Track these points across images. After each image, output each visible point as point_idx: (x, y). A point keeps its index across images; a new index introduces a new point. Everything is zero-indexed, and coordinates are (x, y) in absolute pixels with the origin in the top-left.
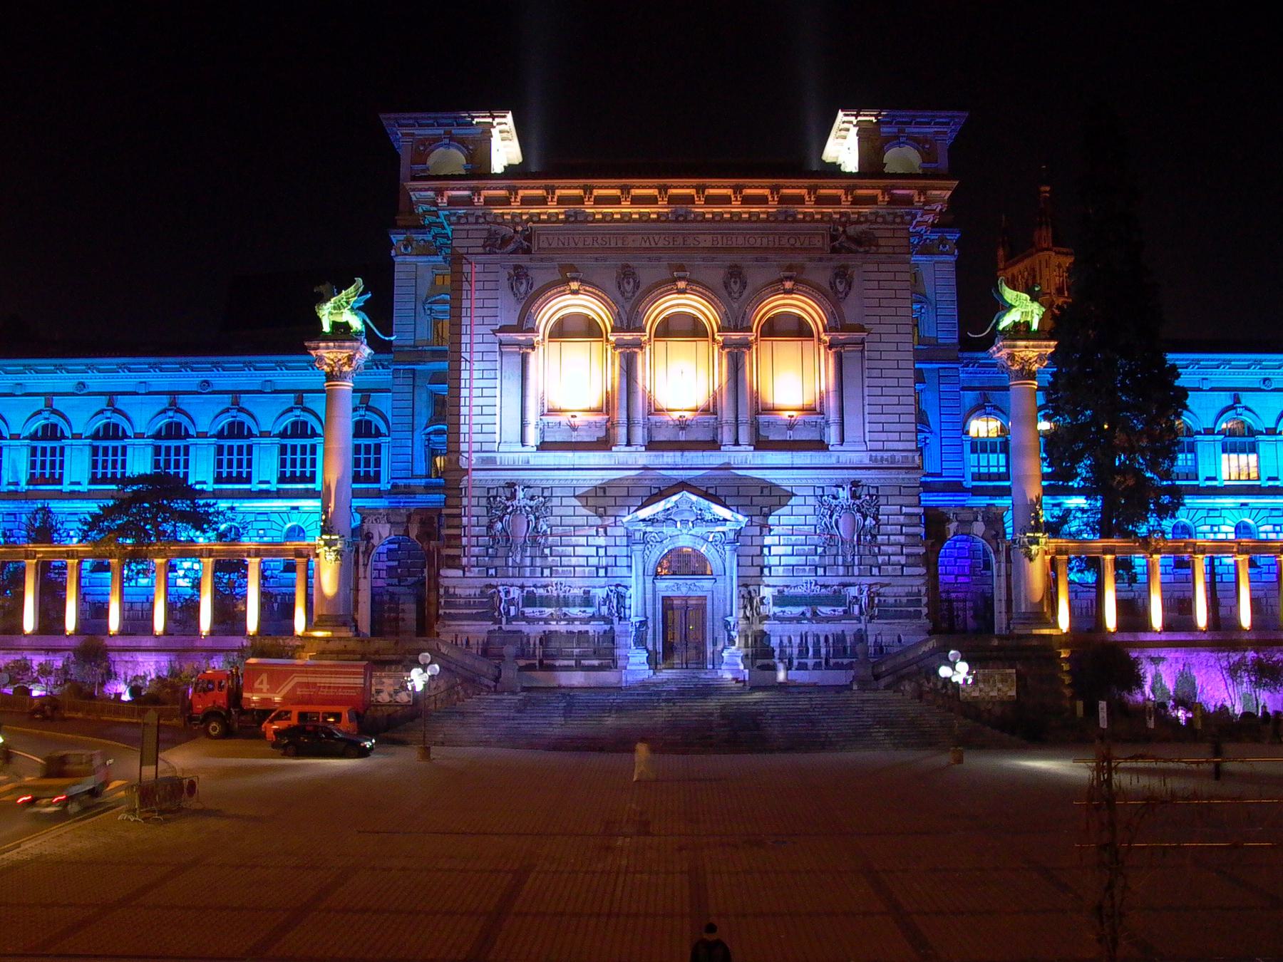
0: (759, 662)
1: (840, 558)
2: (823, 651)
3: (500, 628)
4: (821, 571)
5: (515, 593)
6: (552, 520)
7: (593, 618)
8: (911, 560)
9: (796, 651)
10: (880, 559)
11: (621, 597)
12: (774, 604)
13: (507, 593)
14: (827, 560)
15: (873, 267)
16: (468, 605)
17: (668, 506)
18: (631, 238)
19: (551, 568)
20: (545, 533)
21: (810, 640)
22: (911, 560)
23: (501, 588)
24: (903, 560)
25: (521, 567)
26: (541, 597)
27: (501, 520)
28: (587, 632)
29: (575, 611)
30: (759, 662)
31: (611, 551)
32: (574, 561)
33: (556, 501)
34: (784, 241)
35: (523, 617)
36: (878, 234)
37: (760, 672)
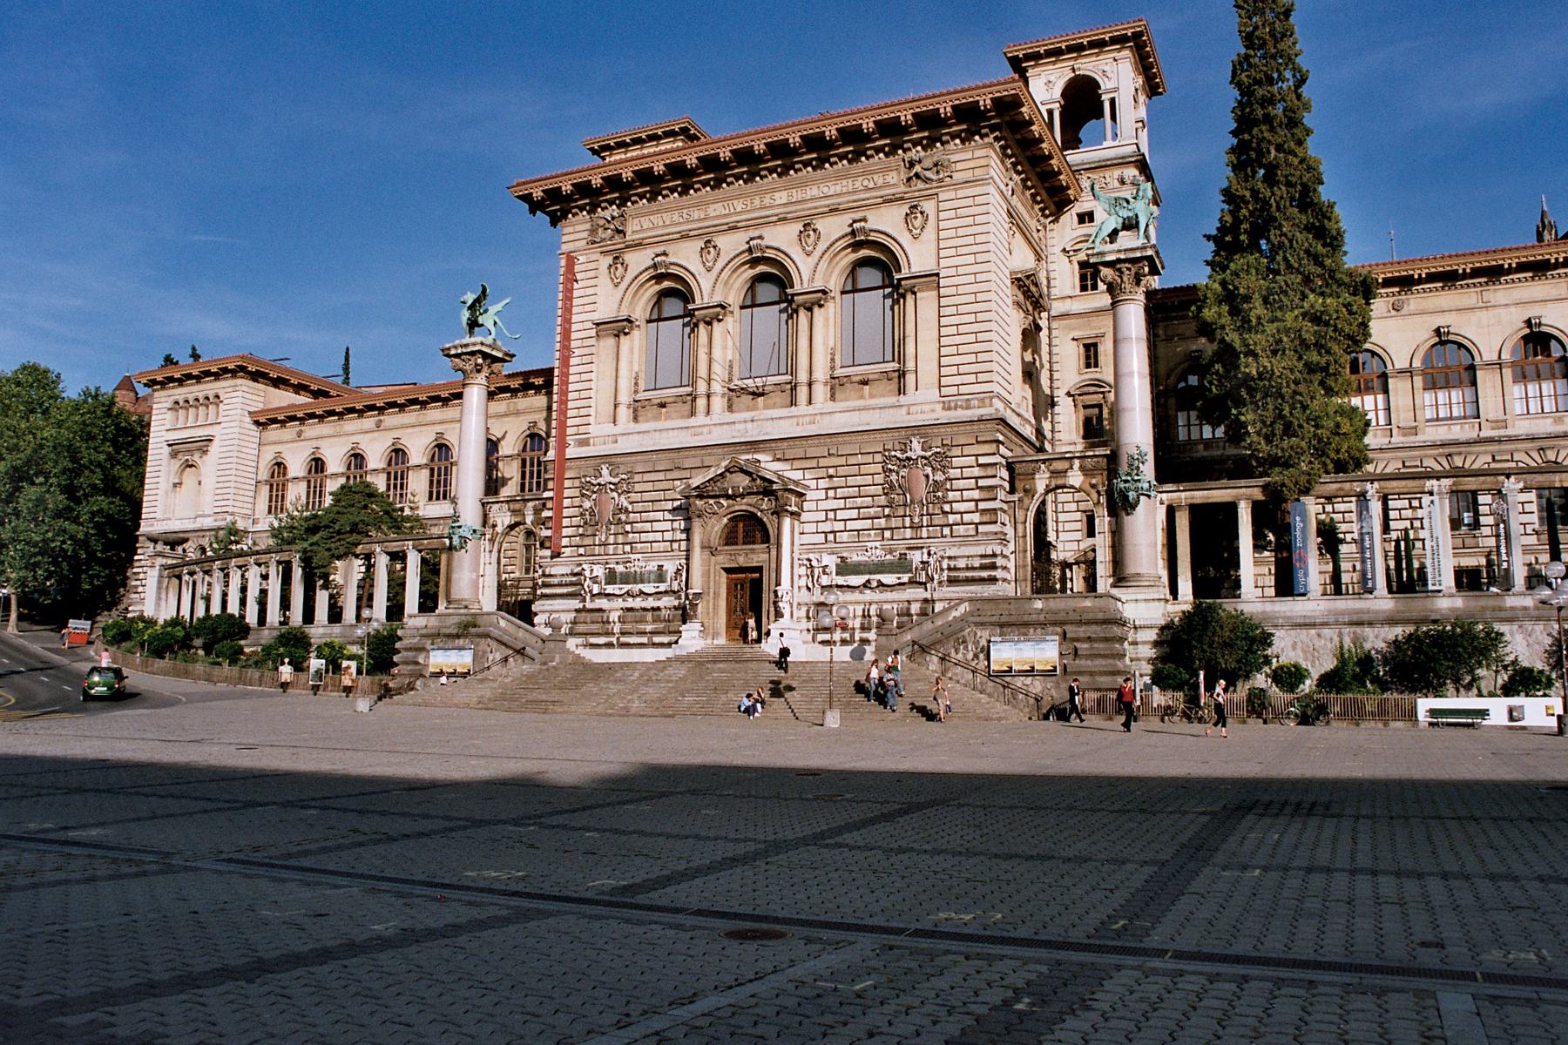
0: (821, 637)
1: (907, 519)
8: (986, 518)
10: (952, 519)
14: (894, 523)
15: (951, 195)
16: (560, 585)
18: (712, 207)
20: (627, 511)
22: (986, 518)
24: (976, 518)
28: (659, 609)
29: (649, 588)
30: (821, 637)
32: (651, 537)
34: (858, 184)
36: (954, 158)
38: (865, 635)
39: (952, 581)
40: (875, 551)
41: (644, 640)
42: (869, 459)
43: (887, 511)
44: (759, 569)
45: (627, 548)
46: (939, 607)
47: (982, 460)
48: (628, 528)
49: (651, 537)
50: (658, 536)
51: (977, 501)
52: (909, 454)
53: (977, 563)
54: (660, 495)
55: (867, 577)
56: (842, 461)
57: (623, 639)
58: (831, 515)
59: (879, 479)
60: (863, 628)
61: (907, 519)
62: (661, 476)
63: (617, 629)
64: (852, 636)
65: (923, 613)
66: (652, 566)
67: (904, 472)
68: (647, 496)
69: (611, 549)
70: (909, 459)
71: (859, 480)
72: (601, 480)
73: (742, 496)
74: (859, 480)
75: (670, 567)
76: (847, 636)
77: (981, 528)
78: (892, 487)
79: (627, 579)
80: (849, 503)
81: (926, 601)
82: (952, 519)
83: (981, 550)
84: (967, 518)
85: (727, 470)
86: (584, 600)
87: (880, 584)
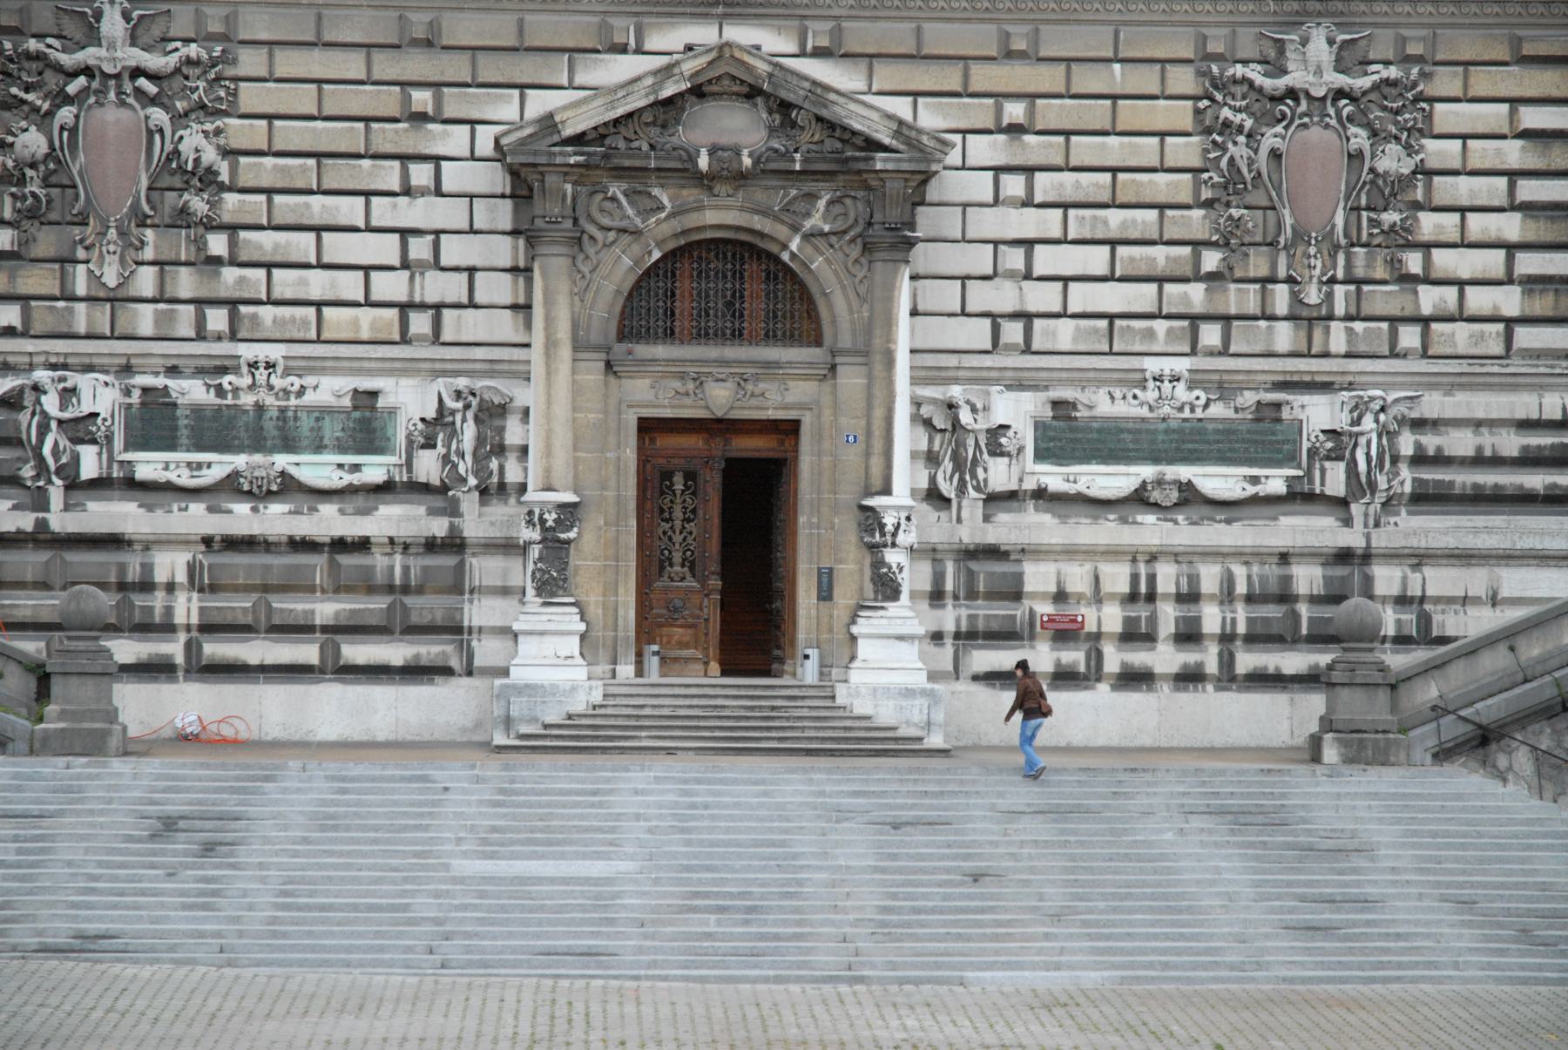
1: (1281, 293)
2: (1211, 618)
3: (42, 525)
4: (1211, 335)
5: (100, 397)
6: (240, 132)
7: (386, 489)
8: (1543, 304)
9: (1112, 618)
10: (1429, 299)
11: (492, 413)
12: (1041, 455)
13: (69, 394)
17: (668, 91)
19: (233, 304)
20: (207, 180)
21: (1167, 577)
22: (1543, 304)
23: (42, 376)
24: (1510, 301)
25: (117, 299)
26: (197, 410)
27: (44, 119)
28: (363, 545)
29: (317, 469)
31: (454, 251)
32: (317, 284)
33: (250, 62)
35: (132, 485)
37: (980, 690)
38: (1139, 657)
39: (1426, 498)
40: (1168, 384)
41: (307, 652)
42: (1146, 79)
43: (1211, 260)
44: (790, 429)
45: (217, 319)
46: (1387, 578)
47: (1533, 118)
48: (217, 244)
49: (317, 284)
50: (350, 284)
51: (1511, 248)
52: (1296, 77)
53: (1511, 443)
54: (348, 136)
55: (1147, 472)
56: (1050, 78)
57: (215, 649)
58: (1014, 259)
59: (1186, 150)
60: (1133, 635)
61: (1281, 293)
62: (352, 65)
63: (187, 608)
64: (1097, 657)
65: (1334, 597)
66: (330, 390)
67: (1271, 138)
68: (291, 134)
69: (145, 318)
70: (1292, 93)
71: (1114, 149)
72: (89, 56)
73: (741, 178)
74: (1114, 149)
75: (410, 400)
76: (1075, 657)
77: (1526, 337)
78: (1233, 184)
79: (216, 430)
80: (1079, 220)
81: (1344, 556)
82: (1429, 299)
83: (1524, 404)
84: (1479, 299)
85: (698, 92)
86: (41, 503)
87: (1189, 496)
